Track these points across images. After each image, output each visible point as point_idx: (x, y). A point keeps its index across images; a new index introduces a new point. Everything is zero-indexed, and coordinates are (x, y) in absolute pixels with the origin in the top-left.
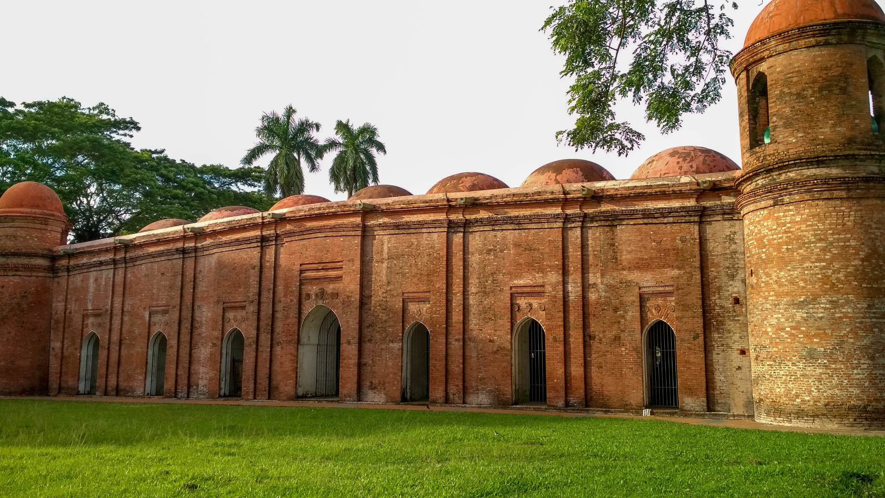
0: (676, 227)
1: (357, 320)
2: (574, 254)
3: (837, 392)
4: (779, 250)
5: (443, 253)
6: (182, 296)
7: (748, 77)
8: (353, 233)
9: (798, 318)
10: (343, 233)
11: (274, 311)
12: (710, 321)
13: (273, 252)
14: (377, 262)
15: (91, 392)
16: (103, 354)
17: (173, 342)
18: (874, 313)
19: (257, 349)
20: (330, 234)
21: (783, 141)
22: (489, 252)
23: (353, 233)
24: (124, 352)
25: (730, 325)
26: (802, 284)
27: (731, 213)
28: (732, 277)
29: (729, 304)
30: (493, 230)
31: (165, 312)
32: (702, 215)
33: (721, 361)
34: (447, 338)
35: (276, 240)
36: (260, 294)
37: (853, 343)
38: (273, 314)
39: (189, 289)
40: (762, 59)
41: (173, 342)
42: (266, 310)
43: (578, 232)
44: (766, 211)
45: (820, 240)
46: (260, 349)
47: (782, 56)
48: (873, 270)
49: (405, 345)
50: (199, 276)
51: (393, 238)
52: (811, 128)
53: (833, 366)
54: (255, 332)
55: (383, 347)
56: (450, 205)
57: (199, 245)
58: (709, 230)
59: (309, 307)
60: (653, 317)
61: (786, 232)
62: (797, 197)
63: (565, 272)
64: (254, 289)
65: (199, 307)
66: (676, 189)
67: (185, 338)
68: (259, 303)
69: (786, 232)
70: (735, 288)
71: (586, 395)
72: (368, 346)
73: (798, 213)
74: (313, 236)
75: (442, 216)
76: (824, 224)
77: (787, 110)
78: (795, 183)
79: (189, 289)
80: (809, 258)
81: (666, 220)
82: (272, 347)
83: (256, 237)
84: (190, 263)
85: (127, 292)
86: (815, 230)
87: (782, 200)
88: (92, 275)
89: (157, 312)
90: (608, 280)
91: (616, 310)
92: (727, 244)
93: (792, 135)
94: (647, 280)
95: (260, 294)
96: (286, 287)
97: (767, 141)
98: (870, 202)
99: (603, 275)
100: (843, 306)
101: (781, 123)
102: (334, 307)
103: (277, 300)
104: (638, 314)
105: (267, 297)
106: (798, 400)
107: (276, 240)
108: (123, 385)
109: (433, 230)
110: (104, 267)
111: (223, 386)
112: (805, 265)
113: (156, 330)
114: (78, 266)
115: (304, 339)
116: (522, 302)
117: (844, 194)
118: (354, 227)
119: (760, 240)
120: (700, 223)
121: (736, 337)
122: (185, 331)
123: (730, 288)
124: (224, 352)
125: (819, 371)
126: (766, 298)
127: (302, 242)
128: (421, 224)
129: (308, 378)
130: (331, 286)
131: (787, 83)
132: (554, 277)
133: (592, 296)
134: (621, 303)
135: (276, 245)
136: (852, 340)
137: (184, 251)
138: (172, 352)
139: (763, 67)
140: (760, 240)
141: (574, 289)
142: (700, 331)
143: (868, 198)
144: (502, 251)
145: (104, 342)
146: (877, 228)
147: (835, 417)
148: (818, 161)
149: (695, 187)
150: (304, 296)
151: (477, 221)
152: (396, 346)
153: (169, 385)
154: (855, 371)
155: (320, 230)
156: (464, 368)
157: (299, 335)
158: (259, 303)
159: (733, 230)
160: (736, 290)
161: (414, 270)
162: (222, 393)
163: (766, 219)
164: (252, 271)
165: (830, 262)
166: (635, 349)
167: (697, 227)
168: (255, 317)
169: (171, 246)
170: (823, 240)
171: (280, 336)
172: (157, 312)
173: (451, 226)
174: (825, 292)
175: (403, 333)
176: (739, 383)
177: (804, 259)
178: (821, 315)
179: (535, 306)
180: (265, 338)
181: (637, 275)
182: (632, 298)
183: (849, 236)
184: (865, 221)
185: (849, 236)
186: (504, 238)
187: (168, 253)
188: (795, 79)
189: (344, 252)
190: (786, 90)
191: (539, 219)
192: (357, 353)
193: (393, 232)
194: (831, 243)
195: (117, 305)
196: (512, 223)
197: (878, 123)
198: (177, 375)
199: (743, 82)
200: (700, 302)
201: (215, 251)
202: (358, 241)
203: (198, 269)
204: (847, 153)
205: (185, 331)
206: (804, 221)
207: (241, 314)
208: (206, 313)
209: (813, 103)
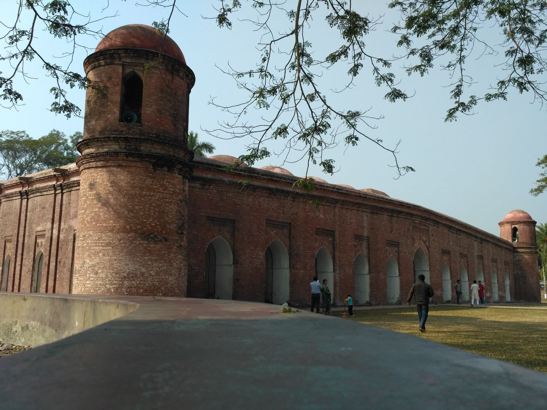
18: (101, 243)
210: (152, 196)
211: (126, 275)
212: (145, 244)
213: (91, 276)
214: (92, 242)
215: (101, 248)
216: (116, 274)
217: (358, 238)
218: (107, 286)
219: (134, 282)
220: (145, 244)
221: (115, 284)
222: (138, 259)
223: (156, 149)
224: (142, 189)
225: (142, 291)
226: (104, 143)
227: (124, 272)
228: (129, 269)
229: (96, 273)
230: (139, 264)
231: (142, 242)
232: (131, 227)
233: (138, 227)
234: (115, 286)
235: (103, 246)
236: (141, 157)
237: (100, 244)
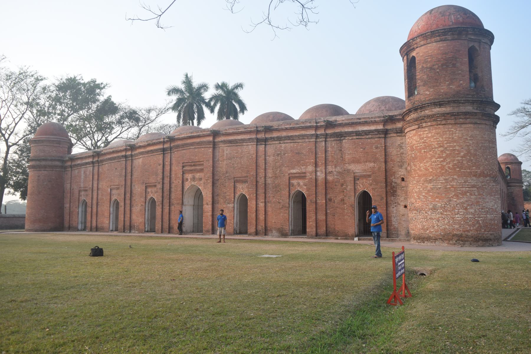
0: (373, 141)
1: (211, 192)
2: (321, 155)
3: (447, 227)
4: (420, 152)
5: (254, 156)
6: (125, 180)
7: (407, 59)
8: (209, 146)
9: (429, 188)
10: (204, 146)
11: (170, 188)
12: (391, 190)
13: (169, 157)
14: (221, 161)
15: (84, 229)
16: (89, 210)
17: (122, 204)
19: (162, 207)
20: (197, 147)
21: (424, 93)
22: (278, 155)
23: (209, 146)
24: (99, 209)
25: (399, 192)
26: (431, 170)
27: (401, 132)
28: (401, 167)
29: (399, 181)
30: (280, 143)
31: (118, 189)
32: (386, 133)
33: (395, 212)
34: (256, 202)
35: (171, 150)
36: (163, 179)
37: (456, 201)
38: (170, 189)
39: (129, 177)
40: (414, 49)
41: (122, 204)
42: (167, 186)
43: (324, 143)
44: (414, 132)
45: (440, 146)
46: (164, 207)
47: (423, 47)
48: (468, 162)
49: (236, 206)
50: (134, 170)
51: (229, 148)
52: (437, 86)
53: (445, 213)
54: (161, 199)
55: (225, 206)
56: (257, 130)
57: (133, 153)
58: (389, 141)
59: (187, 185)
60: (361, 188)
61: (424, 143)
62: (429, 124)
63: (316, 165)
64: (160, 176)
65: (134, 186)
66: (373, 120)
67: (128, 202)
68: (163, 183)
69: (424, 143)
70: (402, 172)
71: (326, 230)
73: (430, 133)
74: (188, 148)
75: (254, 136)
76: (442, 138)
77: (425, 77)
78: (428, 117)
79: (129, 177)
80: (434, 156)
81: (368, 137)
82: (170, 206)
83: (160, 149)
84: (129, 163)
85: (100, 178)
86: (438, 141)
87: (422, 126)
88: (83, 170)
89: (114, 189)
90: (338, 169)
91: (342, 185)
92: (398, 149)
93: (427, 90)
94: (357, 169)
95: (163, 179)
96: (176, 174)
97: (416, 93)
98: (467, 126)
99: (336, 167)
100: (451, 182)
101: (422, 84)
102: (200, 185)
103: (172, 181)
104: (353, 187)
105: (167, 181)
106: (428, 231)
107: (171, 150)
108: (99, 226)
109: (249, 144)
110: (88, 166)
111: (146, 226)
112: (433, 160)
113: (113, 198)
114: (75, 165)
115: (185, 201)
116: (294, 182)
117: (453, 122)
118: (209, 142)
119: (412, 147)
120: (385, 138)
121: (402, 199)
123: (400, 173)
124: (147, 209)
125: (438, 216)
126: (414, 178)
127: (183, 151)
128: (243, 140)
129: (188, 222)
130: (198, 174)
131: (426, 62)
132: (311, 168)
133: (330, 178)
134: (345, 181)
135: (171, 153)
136: (455, 200)
137: (126, 157)
138: (121, 209)
139: (414, 54)
140: (412, 147)
141: (321, 175)
142: (384, 195)
143: (466, 123)
144: (284, 154)
145: (89, 204)
146: (470, 140)
147: (446, 240)
148: (440, 104)
149: (383, 119)
150: (185, 180)
151: (271, 138)
152: (231, 205)
153: (121, 226)
154: (457, 216)
155: (192, 144)
156: (265, 217)
157: (182, 200)
158: (163, 183)
159: (401, 141)
160: (403, 173)
161: (239, 165)
162: (146, 230)
163: (414, 135)
164: (159, 167)
165: (445, 159)
166: (351, 206)
167: (383, 140)
168: (161, 191)
169: (119, 154)
170: (442, 146)
171: (174, 201)
172: (114, 189)
173: (258, 141)
174: (442, 175)
175: (234, 199)
176: (403, 223)
177: (433, 156)
178: (439, 186)
179: (302, 184)
180: (166, 201)
181: (358, 167)
182: (350, 179)
183: (455, 144)
184: (464, 136)
185: (455, 144)
186: (285, 147)
187: (119, 157)
188: (429, 60)
189: (204, 156)
190: (425, 66)
191: (303, 137)
192: (211, 209)
193: (228, 145)
194: (446, 148)
195: (95, 185)
196: (289, 139)
197: (475, 83)
198: (124, 221)
199: (405, 61)
200: (384, 180)
201: (141, 156)
202: (211, 150)
203: (133, 166)
204: (455, 99)
206: (433, 136)
207: (154, 189)
208: (138, 189)
209: (438, 72)
216: (482, 209)
224: (489, 141)
229: (466, 209)
235: (469, 188)
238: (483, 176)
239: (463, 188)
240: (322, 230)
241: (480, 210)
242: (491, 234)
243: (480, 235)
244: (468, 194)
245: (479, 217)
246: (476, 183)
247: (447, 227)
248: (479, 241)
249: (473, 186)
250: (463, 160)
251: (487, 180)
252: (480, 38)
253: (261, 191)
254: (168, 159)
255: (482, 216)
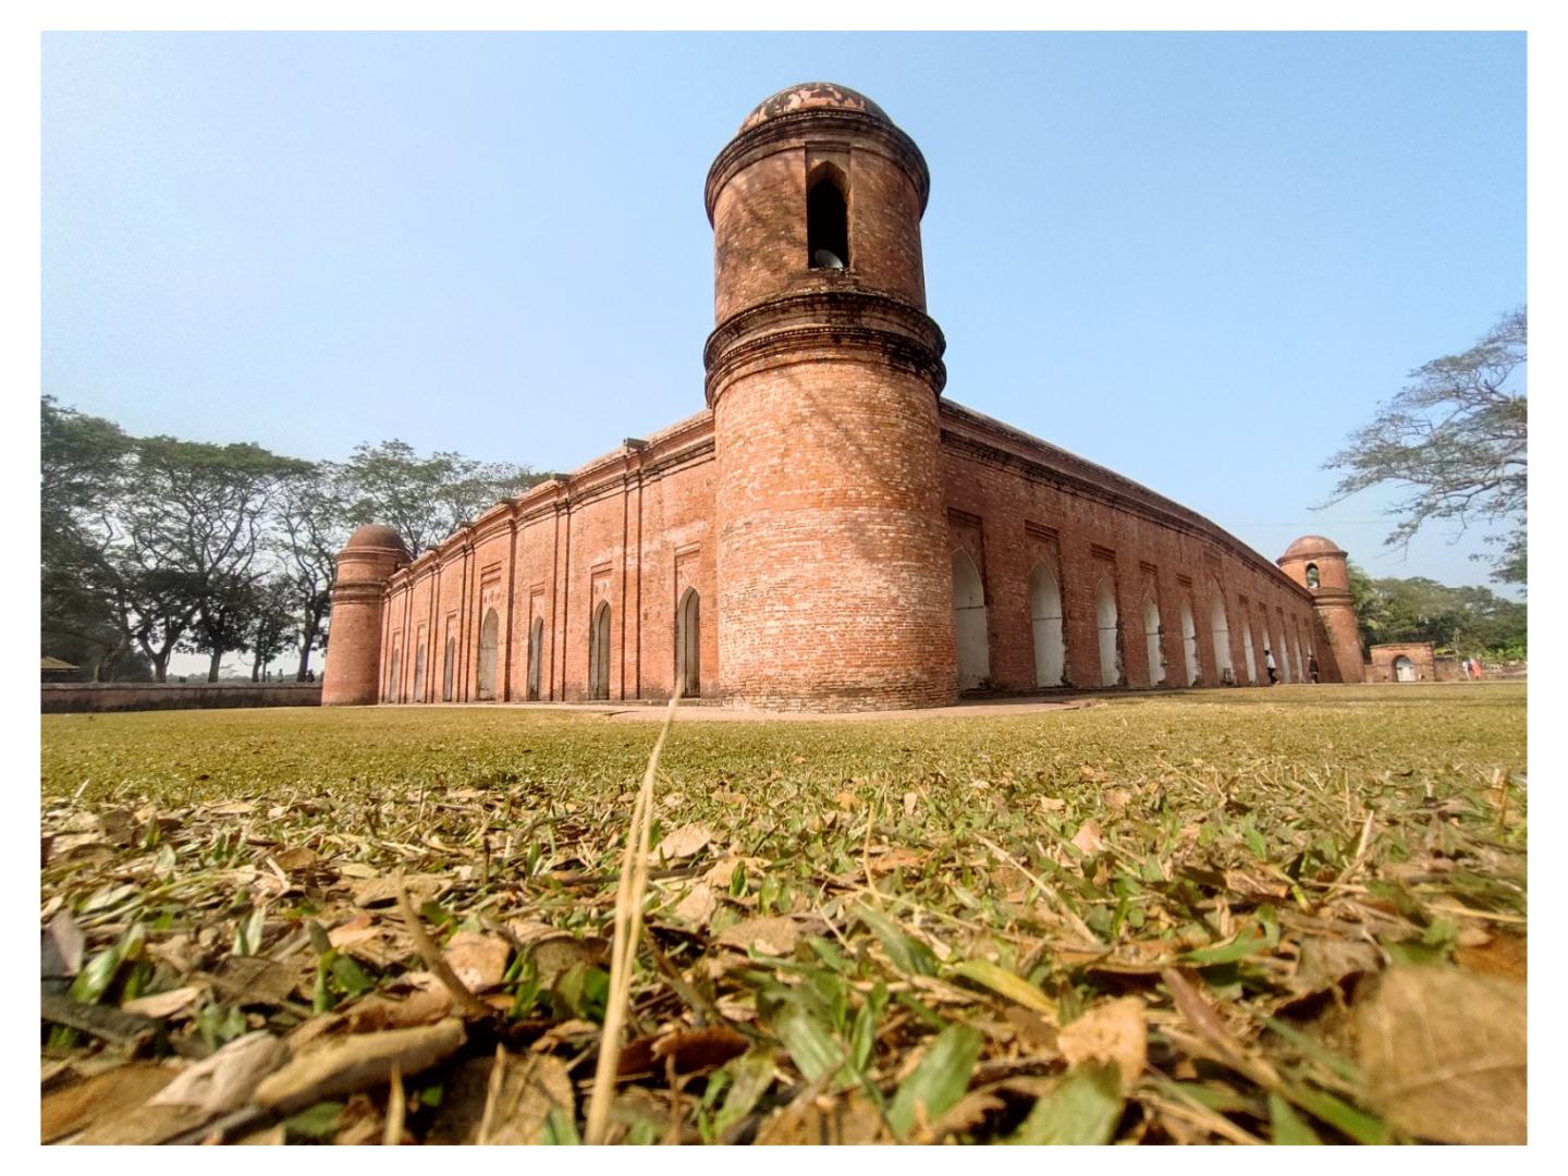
3: (750, 657)
18: (795, 533)
72: (513, 644)
122: (432, 641)
133: (645, 567)
136: (765, 578)
146: (805, 407)
154: (768, 624)
180: (465, 642)
205: (432, 641)
210: (893, 425)
211: (857, 601)
212: (893, 531)
213: (776, 608)
214: (772, 532)
215: (794, 544)
216: (838, 600)
217: (1144, 566)
218: (819, 628)
219: (878, 619)
220: (893, 531)
221: (837, 624)
222: (881, 566)
223: (891, 322)
225: (895, 637)
226: (781, 316)
227: (854, 596)
228: (865, 589)
229: (789, 601)
230: (884, 578)
231: (885, 527)
232: (859, 494)
233: (875, 493)
234: (836, 628)
235: (798, 540)
236: (864, 338)
237: (792, 536)
238: (844, 505)
239: (783, 542)
240: (631, 687)
241: (832, 602)
242: (871, 675)
243: (831, 678)
244: (797, 558)
245: (827, 624)
246: (820, 524)
247: (750, 657)
248: (826, 695)
249: (810, 536)
250: (783, 464)
251: (860, 515)
252: (845, 139)
253: (560, 608)
254: (469, 566)
255: (836, 620)
